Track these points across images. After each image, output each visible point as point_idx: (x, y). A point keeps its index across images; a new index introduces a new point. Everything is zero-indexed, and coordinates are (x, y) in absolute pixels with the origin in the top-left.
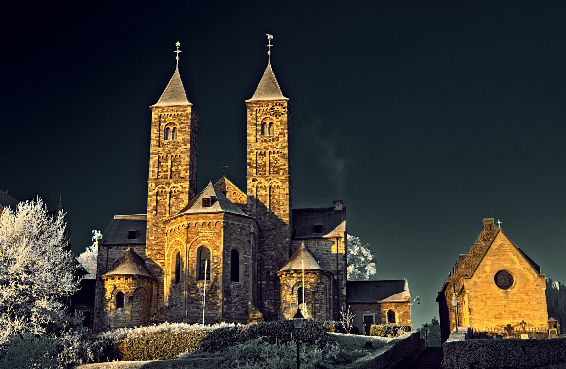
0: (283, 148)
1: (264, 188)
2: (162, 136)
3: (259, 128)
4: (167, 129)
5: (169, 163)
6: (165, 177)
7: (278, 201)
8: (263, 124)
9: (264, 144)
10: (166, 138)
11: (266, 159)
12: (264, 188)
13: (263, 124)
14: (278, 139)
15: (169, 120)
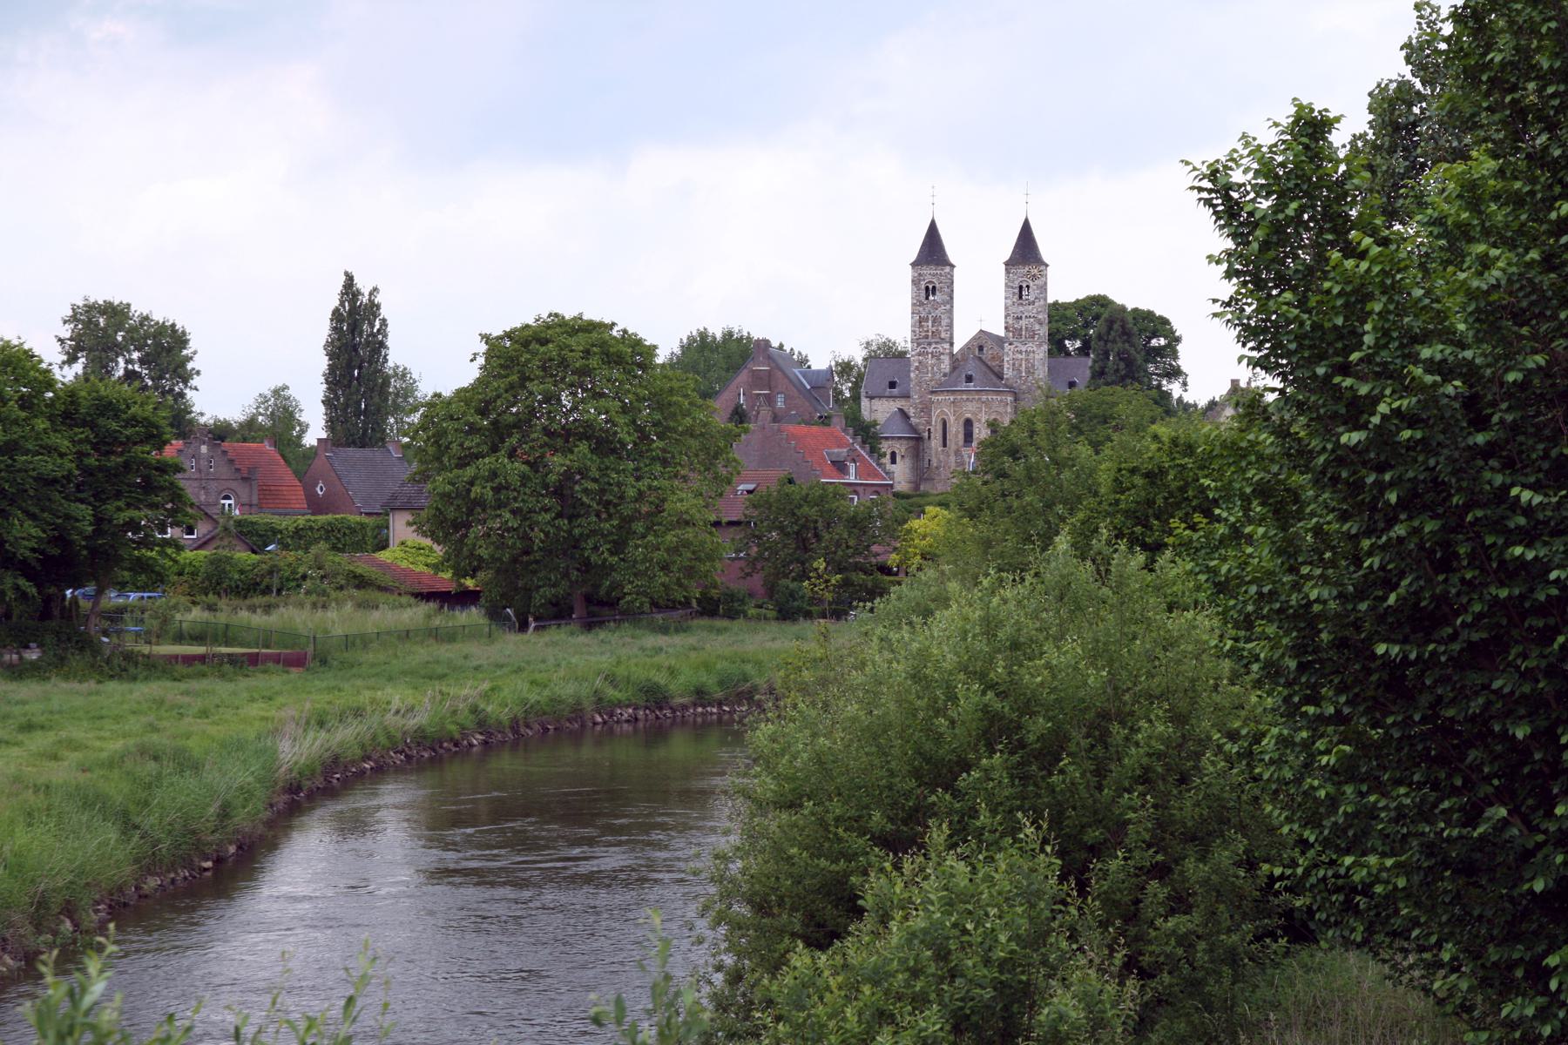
0: (1038, 313)
1: (1021, 352)
2: (923, 293)
3: (1017, 291)
4: (927, 288)
5: (930, 324)
6: (927, 337)
7: (1033, 366)
8: (1021, 287)
9: (1021, 308)
10: (927, 298)
11: (1023, 323)
12: (1021, 352)
13: (1021, 287)
14: (1034, 303)
15: (928, 278)
